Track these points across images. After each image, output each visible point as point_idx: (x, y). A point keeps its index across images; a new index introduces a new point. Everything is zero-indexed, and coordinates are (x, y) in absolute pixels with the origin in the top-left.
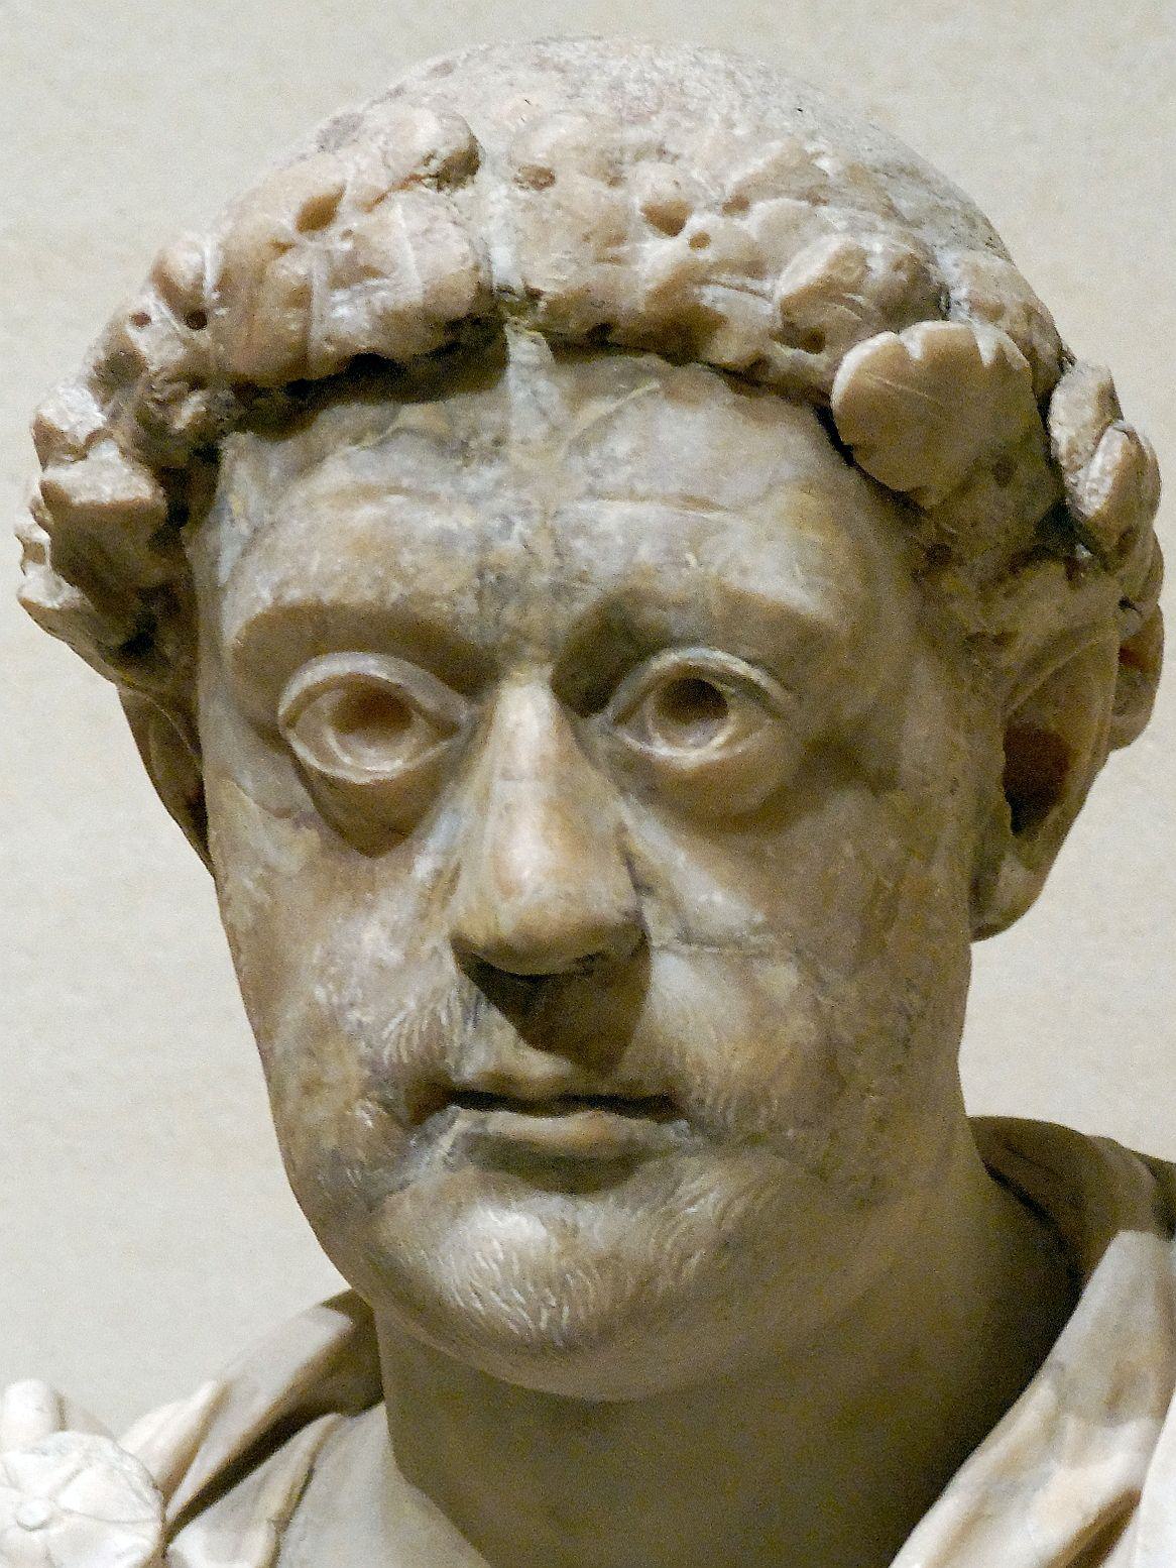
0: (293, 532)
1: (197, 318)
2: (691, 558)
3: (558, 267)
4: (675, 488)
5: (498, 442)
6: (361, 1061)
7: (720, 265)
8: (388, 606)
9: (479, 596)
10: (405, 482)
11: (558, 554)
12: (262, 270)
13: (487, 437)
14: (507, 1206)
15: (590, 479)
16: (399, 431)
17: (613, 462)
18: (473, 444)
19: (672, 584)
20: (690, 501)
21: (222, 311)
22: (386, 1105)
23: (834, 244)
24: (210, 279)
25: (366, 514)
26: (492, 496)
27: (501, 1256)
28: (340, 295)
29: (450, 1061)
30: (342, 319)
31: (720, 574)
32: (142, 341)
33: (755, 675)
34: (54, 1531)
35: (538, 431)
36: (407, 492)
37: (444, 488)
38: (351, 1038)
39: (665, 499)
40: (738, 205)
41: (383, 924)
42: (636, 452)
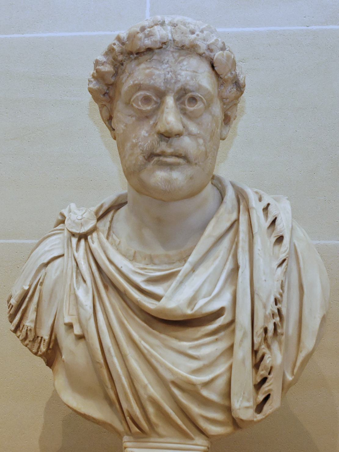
0: (136, 74)
1: (123, 44)
2: (194, 79)
3: (178, 37)
4: (192, 70)
5: (168, 61)
6: (141, 150)
7: (200, 39)
8: (151, 84)
9: (164, 83)
10: (154, 67)
11: (176, 77)
12: (135, 36)
13: (166, 61)
14: (161, 171)
15: (180, 68)
16: (153, 60)
17: (184, 65)
18: (164, 62)
19: (192, 83)
20: (194, 72)
21: (127, 42)
22: (144, 157)
23: (215, 38)
24: (125, 38)
25: (148, 71)
26: (167, 69)
27: (161, 178)
28: (146, 39)
29: (155, 150)
30: (146, 43)
31: (198, 82)
32: (115, 47)
33: (202, 97)
34: (82, 220)
35: (173, 60)
36: (154, 68)
37: (160, 68)
38: (139, 147)
39: (191, 71)
40: (202, 31)
41: (145, 130)
42: (187, 64)
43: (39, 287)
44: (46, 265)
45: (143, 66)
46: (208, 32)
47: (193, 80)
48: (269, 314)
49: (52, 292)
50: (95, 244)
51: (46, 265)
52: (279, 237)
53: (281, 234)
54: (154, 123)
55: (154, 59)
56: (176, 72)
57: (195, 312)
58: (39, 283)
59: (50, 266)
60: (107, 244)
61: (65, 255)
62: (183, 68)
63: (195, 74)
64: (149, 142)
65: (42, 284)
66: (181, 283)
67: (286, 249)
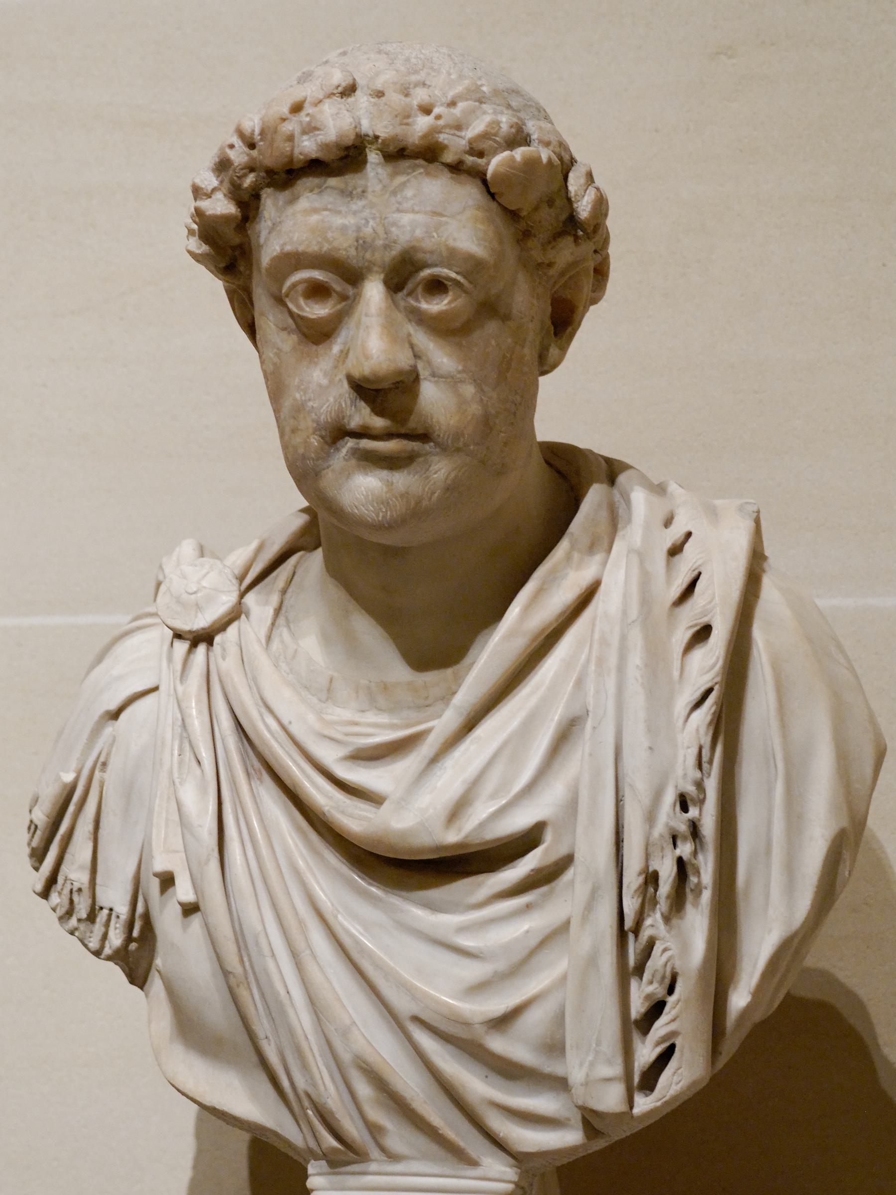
1: (252, 146)
2: (435, 234)
3: (386, 127)
4: (429, 209)
5: (363, 192)
6: (313, 421)
7: (446, 126)
9: (357, 249)
10: (329, 206)
13: (359, 190)
14: (367, 474)
16: (327, 187)
17: (406, 199)
18: (354, 192)
19: (428, 244)
20: (435, 213)
21: (261, 143)
22: (322, 437)
23: (488, 118)
24: (257, 131)
25: (314, 218)
26: (361, 211)
28: (305, 137)
29: (346, 421)
31: (446, 240)
32: (232, 154)
33: (459, 278)
34: (199, 595)
35: (378, 188)
37: (343, 209)
38: (309, 412)
39: (426, 213)
40: (452, 104)
41: (321, 370)
42: (414, 196)
43: (97, 774)
44: (115, 715)
45: (304, 203)
46: (470, 102)
47: (433, 237)
48: (661, 836)
49: (129, 791)
50: (227, 660)
51: (115, 715)
52: (698, 628)
53: (704, 620)
54: (342, 351)
55: (331, 188)
56: (386, 218)
57: (467, 837)
58: (98, 765)
59: (123, 716)
60: (263, 662)
61: (161, 688)
62: (406, 205)
63: (440, 217)
64: (332, 400)
65: (104, 764)
66: (435, 760)
67: (714, 659)
